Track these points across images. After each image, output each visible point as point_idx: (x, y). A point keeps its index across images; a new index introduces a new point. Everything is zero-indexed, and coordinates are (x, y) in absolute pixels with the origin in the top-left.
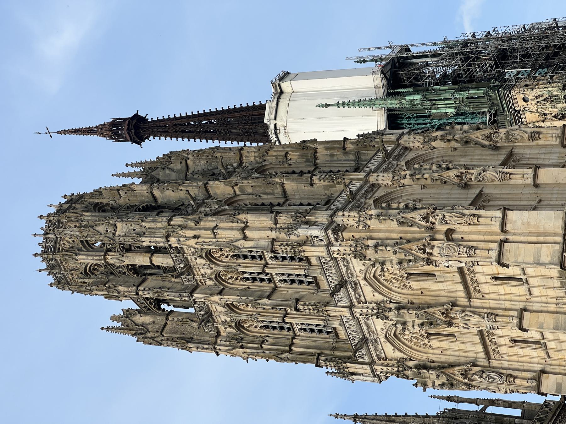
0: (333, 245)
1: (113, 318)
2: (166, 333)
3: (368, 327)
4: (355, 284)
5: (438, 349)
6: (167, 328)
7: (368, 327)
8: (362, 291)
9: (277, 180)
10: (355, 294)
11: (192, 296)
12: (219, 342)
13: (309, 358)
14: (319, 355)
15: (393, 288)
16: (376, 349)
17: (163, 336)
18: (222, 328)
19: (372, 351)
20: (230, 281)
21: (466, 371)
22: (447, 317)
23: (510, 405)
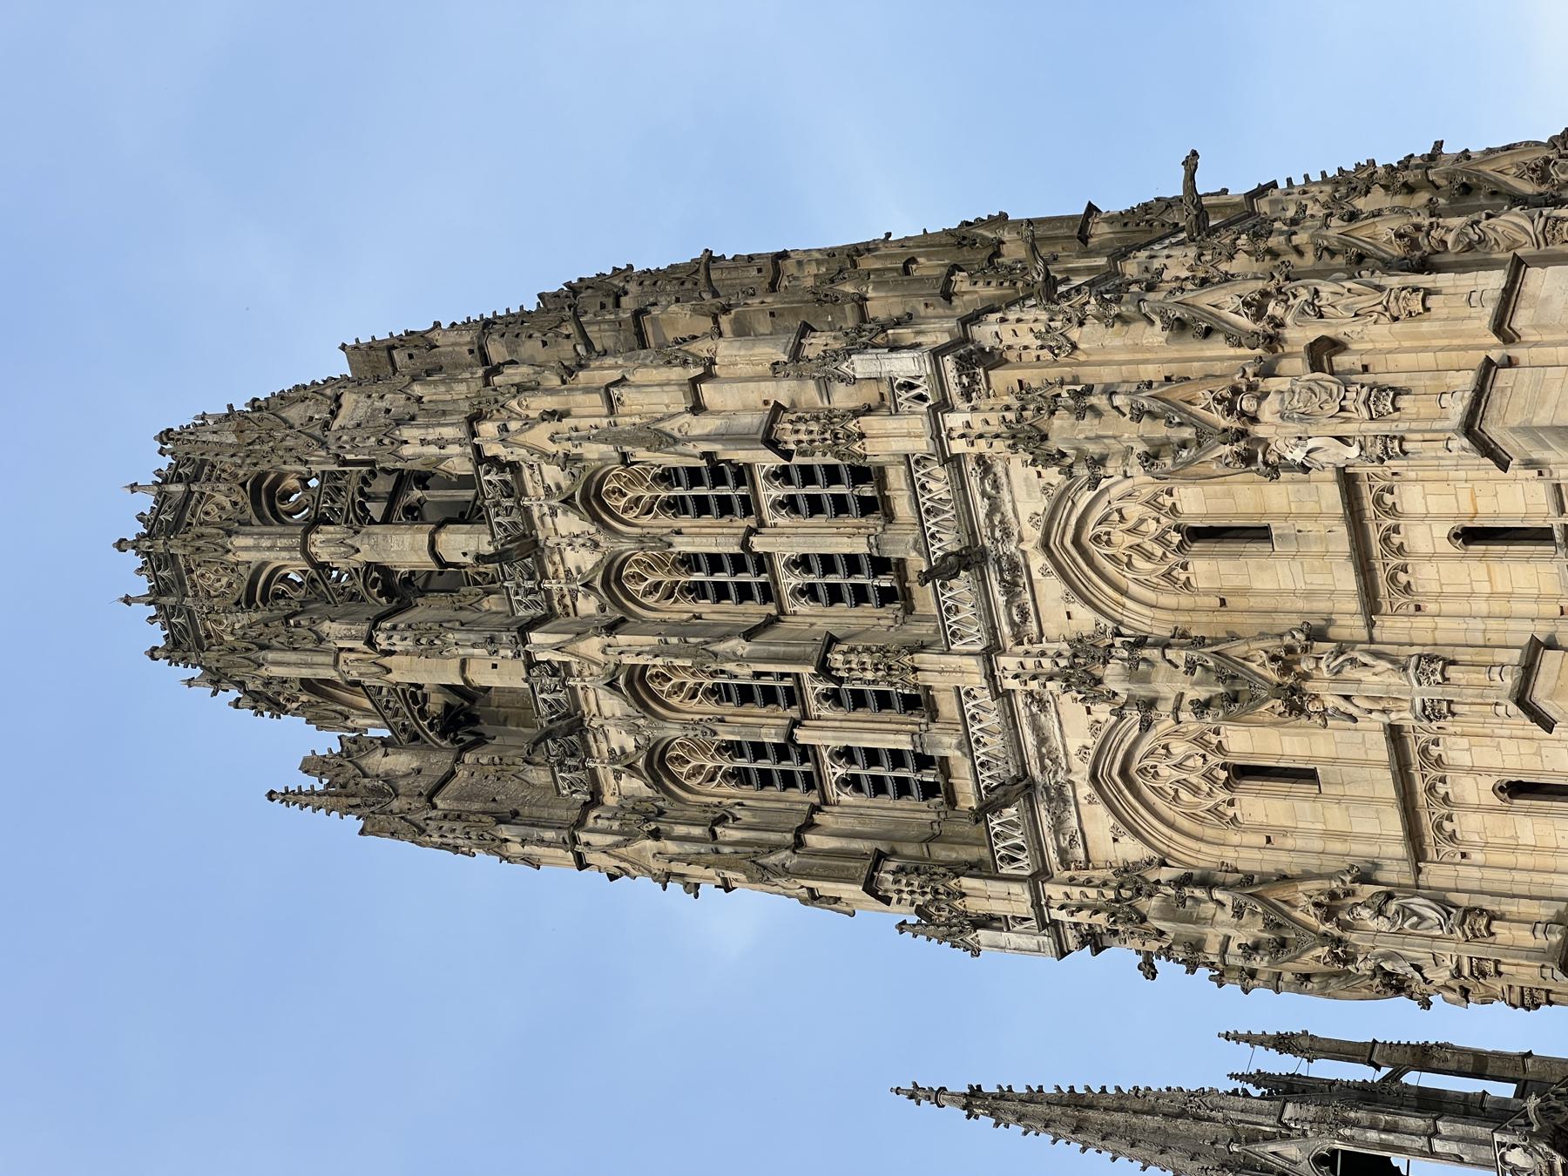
0: (952, 410)
1: (307, 767)
2: (444, 799)
3: (1042, 740)
4: (1014, 567)
5: (1256, 829)
6: (453, 785)
7: (1042, 740)
8: (1034, 600)
9: (849, 288)
10: (1008, 603)
11: (525, 641)
12: (590, 822)
13: (848, 868)
14: (880, 857)
15: (1135, 589)
16: (1058, 827)
17: (434, 807)
18: (605, 773)
19: (1046, 830)
20: (649, 601)
21: (1333, 895)
22: (1286, 669)
23: (1480, 1064)
